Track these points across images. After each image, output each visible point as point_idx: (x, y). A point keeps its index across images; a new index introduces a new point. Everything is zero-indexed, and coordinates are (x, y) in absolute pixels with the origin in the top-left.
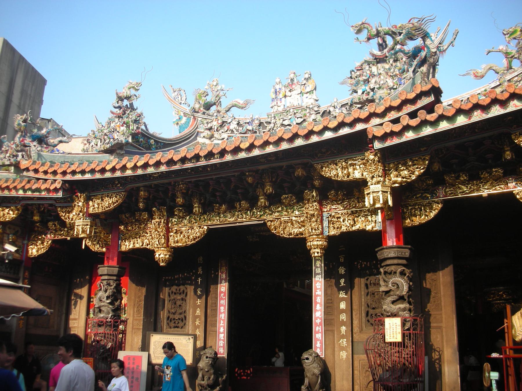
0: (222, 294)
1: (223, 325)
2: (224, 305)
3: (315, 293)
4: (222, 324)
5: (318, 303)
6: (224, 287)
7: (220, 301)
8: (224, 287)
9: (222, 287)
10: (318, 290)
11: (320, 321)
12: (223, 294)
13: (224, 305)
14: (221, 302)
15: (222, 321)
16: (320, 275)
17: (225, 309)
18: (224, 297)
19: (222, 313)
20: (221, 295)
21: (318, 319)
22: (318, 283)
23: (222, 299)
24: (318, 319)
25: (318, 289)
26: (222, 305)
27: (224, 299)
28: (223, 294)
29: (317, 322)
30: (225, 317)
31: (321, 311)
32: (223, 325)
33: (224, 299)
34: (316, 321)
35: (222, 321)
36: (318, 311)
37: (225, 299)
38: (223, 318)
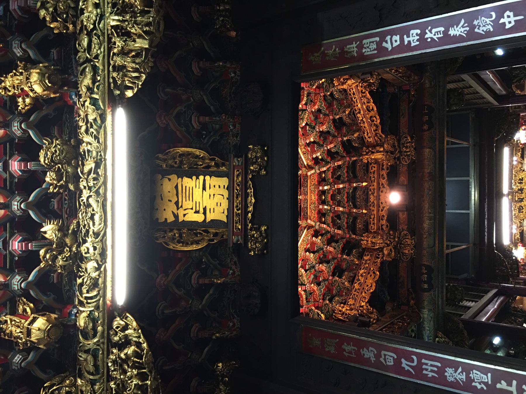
0: (404, 363)
1: (514, 383)
2: (439, 365)
3: (416, 48)
4: (510, 384)
5: (446, 32)
6: (383, 352)
7: (425, 378)
8: (383, 352)
9: (382, 360)
10: (406, 40)
11: (511, 14)
12: (403, 360)
13: (439, 365)
14: (431, 374)
15: (498, 386)
16: (365, 41)
17: (455, 366)
18: (413, 361)
19: (470, 380)
20: (407, 368)
21: (502, 21)
22: (384, 44)
23: (419, 368)
24: (502, 21)
25: (402, 40)
26: (441, 372)
27: (419, 361)
28: (403, 360)
29: (513, 23)
30: (485, 371)
31: (476, 15)
32: (514, 383)
33: (420, 363)
34: (508, 26)
35: (498, 386)
36: (472, 27)
37: (420, 357)
38: (488, 378)
